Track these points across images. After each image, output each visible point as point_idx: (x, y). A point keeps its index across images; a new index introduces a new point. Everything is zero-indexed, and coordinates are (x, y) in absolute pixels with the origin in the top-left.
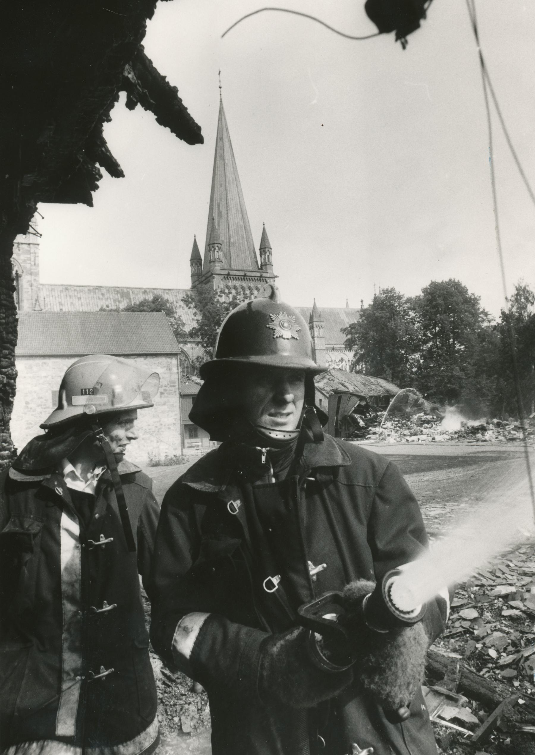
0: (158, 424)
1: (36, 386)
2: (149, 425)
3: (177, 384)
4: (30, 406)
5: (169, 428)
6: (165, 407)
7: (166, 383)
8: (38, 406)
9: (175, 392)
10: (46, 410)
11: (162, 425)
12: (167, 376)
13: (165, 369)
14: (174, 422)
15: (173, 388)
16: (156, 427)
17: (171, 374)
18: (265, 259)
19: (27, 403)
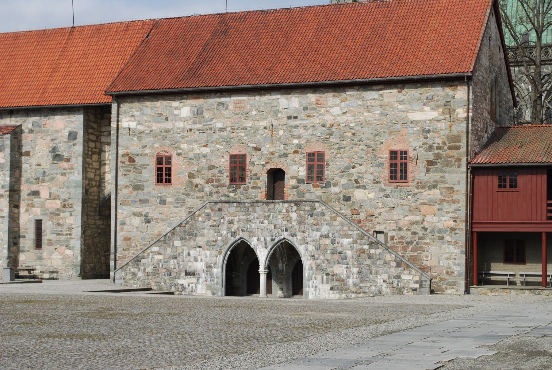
0: (418, 229)
1: (205, 146)
2: (400, 229)
3: (463, 144)
4: (196, 181)
5: (442, 238)
6: (436, 193)
7: (440, 141)
8: (207, 182)
9: (459, 160)
10: (220, 189)
11: (426, 229)
13: (441, 110)
14: (452, 224)
15: (455, 153)
16: (415, 233)
19: (191, 176)
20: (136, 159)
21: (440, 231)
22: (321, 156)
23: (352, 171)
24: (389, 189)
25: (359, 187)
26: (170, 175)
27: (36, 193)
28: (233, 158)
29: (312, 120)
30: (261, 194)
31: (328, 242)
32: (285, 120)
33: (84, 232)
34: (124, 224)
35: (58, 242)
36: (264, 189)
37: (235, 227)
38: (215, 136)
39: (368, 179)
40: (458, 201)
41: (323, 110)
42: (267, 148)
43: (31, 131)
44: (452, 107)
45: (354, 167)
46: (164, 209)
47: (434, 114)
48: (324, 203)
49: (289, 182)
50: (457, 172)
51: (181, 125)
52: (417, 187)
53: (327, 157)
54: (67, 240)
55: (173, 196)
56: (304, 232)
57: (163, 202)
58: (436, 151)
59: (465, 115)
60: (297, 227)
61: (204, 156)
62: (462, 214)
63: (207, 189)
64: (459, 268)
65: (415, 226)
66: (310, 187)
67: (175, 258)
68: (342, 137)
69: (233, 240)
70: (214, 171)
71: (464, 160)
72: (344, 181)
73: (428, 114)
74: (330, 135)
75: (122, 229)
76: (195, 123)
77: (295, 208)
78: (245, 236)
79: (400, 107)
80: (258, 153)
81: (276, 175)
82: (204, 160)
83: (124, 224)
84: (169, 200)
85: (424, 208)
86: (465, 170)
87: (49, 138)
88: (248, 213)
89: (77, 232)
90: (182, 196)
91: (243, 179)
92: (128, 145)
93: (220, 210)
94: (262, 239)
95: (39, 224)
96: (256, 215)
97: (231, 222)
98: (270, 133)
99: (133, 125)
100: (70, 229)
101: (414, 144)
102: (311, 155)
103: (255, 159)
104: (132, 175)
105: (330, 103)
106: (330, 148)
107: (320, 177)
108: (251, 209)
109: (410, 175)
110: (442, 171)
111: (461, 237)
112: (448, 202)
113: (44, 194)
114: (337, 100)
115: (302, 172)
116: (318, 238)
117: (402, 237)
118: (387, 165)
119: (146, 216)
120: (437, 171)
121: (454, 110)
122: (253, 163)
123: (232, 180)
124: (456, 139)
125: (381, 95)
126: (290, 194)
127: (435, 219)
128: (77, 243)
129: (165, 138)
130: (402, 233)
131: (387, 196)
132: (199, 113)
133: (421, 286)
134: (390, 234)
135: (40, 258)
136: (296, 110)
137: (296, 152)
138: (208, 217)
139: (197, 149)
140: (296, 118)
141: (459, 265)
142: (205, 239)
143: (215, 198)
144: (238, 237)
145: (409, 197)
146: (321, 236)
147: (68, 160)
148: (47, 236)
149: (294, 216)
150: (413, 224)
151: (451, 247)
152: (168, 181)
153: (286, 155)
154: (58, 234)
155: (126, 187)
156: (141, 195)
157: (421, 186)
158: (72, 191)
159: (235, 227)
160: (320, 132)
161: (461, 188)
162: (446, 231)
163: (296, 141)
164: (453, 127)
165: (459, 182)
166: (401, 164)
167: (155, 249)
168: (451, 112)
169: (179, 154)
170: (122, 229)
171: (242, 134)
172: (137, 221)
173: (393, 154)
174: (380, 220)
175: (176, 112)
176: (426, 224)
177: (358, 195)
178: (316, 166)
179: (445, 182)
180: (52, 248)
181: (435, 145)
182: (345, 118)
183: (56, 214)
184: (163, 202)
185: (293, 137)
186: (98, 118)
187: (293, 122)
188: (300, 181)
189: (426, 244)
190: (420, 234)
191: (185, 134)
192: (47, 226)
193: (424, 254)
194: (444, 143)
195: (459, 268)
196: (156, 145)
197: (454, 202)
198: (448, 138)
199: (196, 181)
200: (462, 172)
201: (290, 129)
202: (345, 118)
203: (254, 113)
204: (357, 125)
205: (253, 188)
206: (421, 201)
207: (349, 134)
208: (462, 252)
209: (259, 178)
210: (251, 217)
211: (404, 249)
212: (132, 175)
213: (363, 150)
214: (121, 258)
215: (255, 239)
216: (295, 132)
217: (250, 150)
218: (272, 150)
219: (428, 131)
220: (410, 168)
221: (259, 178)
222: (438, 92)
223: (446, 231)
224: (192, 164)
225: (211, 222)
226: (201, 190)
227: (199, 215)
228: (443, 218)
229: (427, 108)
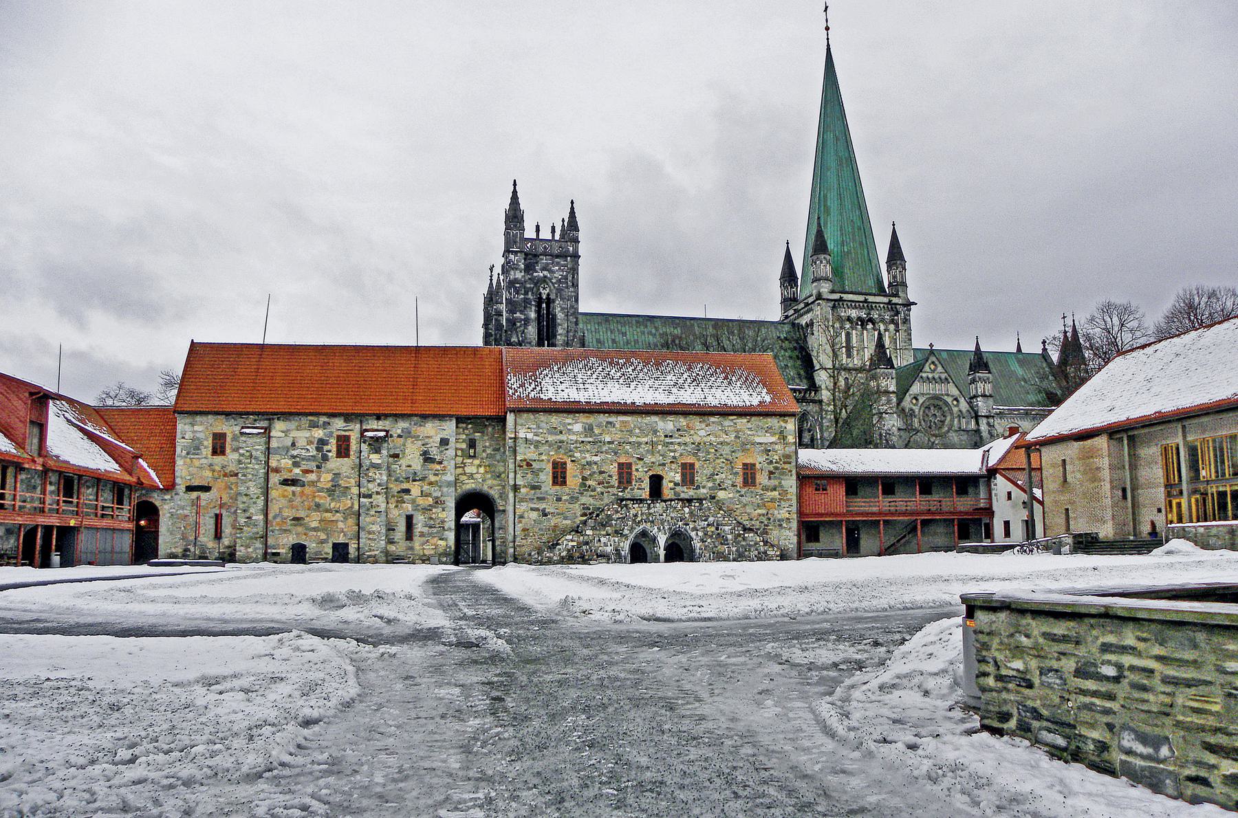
0: (764, 519)
4: (588, 483)
14: (787, 515)
15: (787, 466)
18: (895, 277)
19: (584, 479)
20: (535, 465)
22: (692, 465)
24: (743, 491)
26: (565, 478)
27: (407, 491)
30: (645, 494)
31: (713, 529)
34: (522, 517)
35: (430, 534)
36: (648, 490)
42: (649, 459)
43: (400, 436)
46: (560, 504)
47: (773, 439)
49: (667, 486)
51: (574, 438)
53: (697, 466)
57: (559, 499)
62: (794, 509)
67: (587, 543)
68: (709, 453)
71: (794, 472)
72: (710, 484)
81: (656, 481)
88: (649, 508)
91: (629, 482)
95: (409, 519)
97: (636, 516)
99: (530, 436)
100: (443, 522)
102: (684, 466)
107: (692, 482)
111: (794, 525)
113: (415, 490)
114: (703, 426)
115: (678, 478)
119: (544, 510)
124: (788, 456)
126: (667, 492)
132: (589, 429)
135: (411, 548)
139: (589, 458)
147: (440, 463)
148: (419, 527)
153: (664, 465)
156: (538, 493)
158: (445, 489)
161: (794, 490)
167: (569, 537)
168: (784, 438)
172: (534, 515)
177: (721, 495)
178: (688, 472)
182: (708, 439)
184: (559, 499)
187: (668, 440)
188: (676, 484)
199: (588, 483)
201: (666, 445)
202: (708, 439)
216: (671, 447)
222: (773, 422)
225: (619, 515)
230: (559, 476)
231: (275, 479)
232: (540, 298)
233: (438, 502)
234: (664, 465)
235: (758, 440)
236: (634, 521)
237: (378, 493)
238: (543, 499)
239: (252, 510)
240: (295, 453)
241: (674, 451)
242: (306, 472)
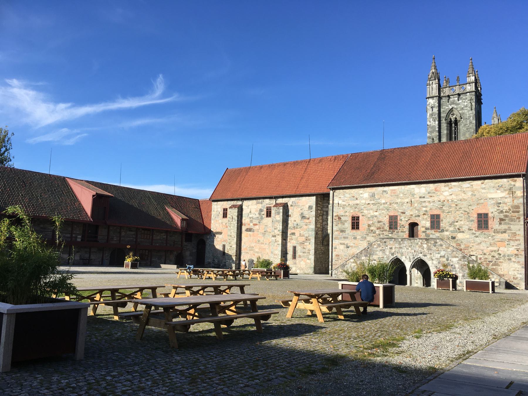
2: (485, 254)
4: (372, 228)
5: (510, 259)
6: (506, 236)
8: (377, 229)
9: (519, 218)
11: (500, 254)
12: (509, 200)
13: (507, 192)
15: (516, 214)
16: (493, 257)
17: (514, 198)
19: (369, 226)
20: (342, 218)
21: (508, 256)
22: (438, 216)
23: (456, 224)
24: (478, 233)
25: (460, 232)
26: (358, 225)
28: (391, 217)
29: (433, 198)
30: (406, 235)
32: (418, 199)
33: (315, 252)
34: (336, 248)
36: (407, 232)
37: (393, 251)
38: (381, 207)
39: (465, 228)
40: (519, 240)
41: (439, 193)
42: (408, 213)
43: (292, 206)
44: (514, 190)
45: (457, 222)
48: (442, 240)
49: (420, 229)
50: (518, 225)
51: (363, 201)
52: (494, 232)
53: (441, 217)
54: (307, 255)
55: (360, 235)
56: (431, 254)
57: (355, 238)
58: (505, 214)
59: (522, 194)
60: (427, 252)
61: (376, 216)
62: (522, 247)
63: (377, 232)
64: (521, 276)
65: (493, 252)
66: (433, 231)
68: (450, 207)
69: (392, 257)
70: (381, 223)
72: (451, 229)
73: (499, 194)
74: (443, 205)
75: (335, 251)
76: (371, 200)
77: (426, 242)
78: (399, 256)
79: (483, 191)
80: (404, 215)
81: (413, 226)
82: (376, 218)
83: (336, 248)
84: (358, 237)
85: (498, 243)
86: (523, 223)
87: (299, 209)
89: (312, 252)
90: (365, 236)
91: (396, 228)
92: (337, 211)
93: (385, 242)
94: (408, 257)
95: (295, 248)
96: (404, 245)
97: (391, 248)
98: (410, 205)
99: (340, 202)
100: (309, 250)
101: (491, 210)
103: (402, 218)
104: (340, 225)
105: (442, 190)
106: (443, 212)
107: (438, 227)
108: (401, 242)
109: (490, 226)
110: (509, 224)
112: (513, 240)
113: (297, 234)
114: (447, 188)
115: (428, 224)
116: (439, 257)
117: (486, 258)
118: (476, 221)
120: (505, 224)
121: (515, 192)
122: (401, 220)
123: (390, 228)
124: (517, 207)
125: (472, 185)
126: (422, 235)
127: (505, 249)
128: (312, 257)
129: (356, 208)
130: (486, 256)
131: (477, 237)
132: (373, 195)
133: (500, 284)
134: (479, 256)
135: (295, 263)
136: (424, 194)
137: (424, 214)
138: (379, 245)
139: (372, 213)
140: (424, 197)
141: (521, 274)
142: (378, 257)
143: (382, 236)
144: (395, 256)
145: (490, 237)
146: (441, 257)
147: (308, 219)
149: (425, 246)
150: (492, 252)
151: (516, 264)
152: (358, 228)
154: (304, 253)
155: (337, 231)
156: (344, 234)
157: (496, 232)
158: (310, 233)
159: (393, 251)
160: (437, 204)
162: (512, 256)
163: (424, 209)
164: (515, 201)
165: (519, 230)
166: (484, 221)
167: (352, 260)
169: (363, 215)
170: (335, 251)
171: (395, 206)
172: (342, 247)
173: (479, 215)
174: (473, 249)
175: (361, 195)
176: (500, 252)
177: (460, 236)
178: (435, 221)
179: (510, 230)
180: (300, 259)
181: (504, 211)
183: (302, 243)
184: (355, 238)
185: (423, 207)
186: (323, 199)
188: (427, 229)
189: (500, 262)
190: (497, 257)
191: (366, 206)
192: (298, 249)
193: (499, 267)
194: (510, 209)
195: (521, 276)
196: (352, 211)
197: (517, 240)
198: (512, 207)
199: (372, 228)
200: (521, 225)
203: (401, 195)
204: (458, 200)
205: (401, 232)
206: (497, 240)
207: (454, 205)
208: (522, 267)
209: (404, 227)
210: (402, 246)
211: (488, 264)
212: (340, 225)
213: (462, 213)
214: (334, 264)
215: (404, 257)
216: (424, 204)
217: (399, 213)
218: (411, 213)
219: (500, 203)
220: (490, 222)
221: (404, 227)
223: (512, 256)
224: (370, 220)
225: (380, 248)
226: (375, 233)
227: (375, 245)
228: (510, 249)
229: (498, 191)
230: (355, 224)
231: (244, 228)
232: (451, 121)
233: (307, 239)
234: (419, 216)
235: (490, 196)
236: (390, 252)
237: (278, 235)
238: (347, 238)
239: (232, 243)
240: (251, 216)
241: (426, 207)
242: (255, 225)
